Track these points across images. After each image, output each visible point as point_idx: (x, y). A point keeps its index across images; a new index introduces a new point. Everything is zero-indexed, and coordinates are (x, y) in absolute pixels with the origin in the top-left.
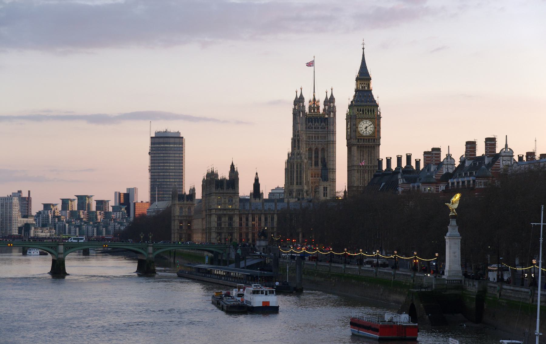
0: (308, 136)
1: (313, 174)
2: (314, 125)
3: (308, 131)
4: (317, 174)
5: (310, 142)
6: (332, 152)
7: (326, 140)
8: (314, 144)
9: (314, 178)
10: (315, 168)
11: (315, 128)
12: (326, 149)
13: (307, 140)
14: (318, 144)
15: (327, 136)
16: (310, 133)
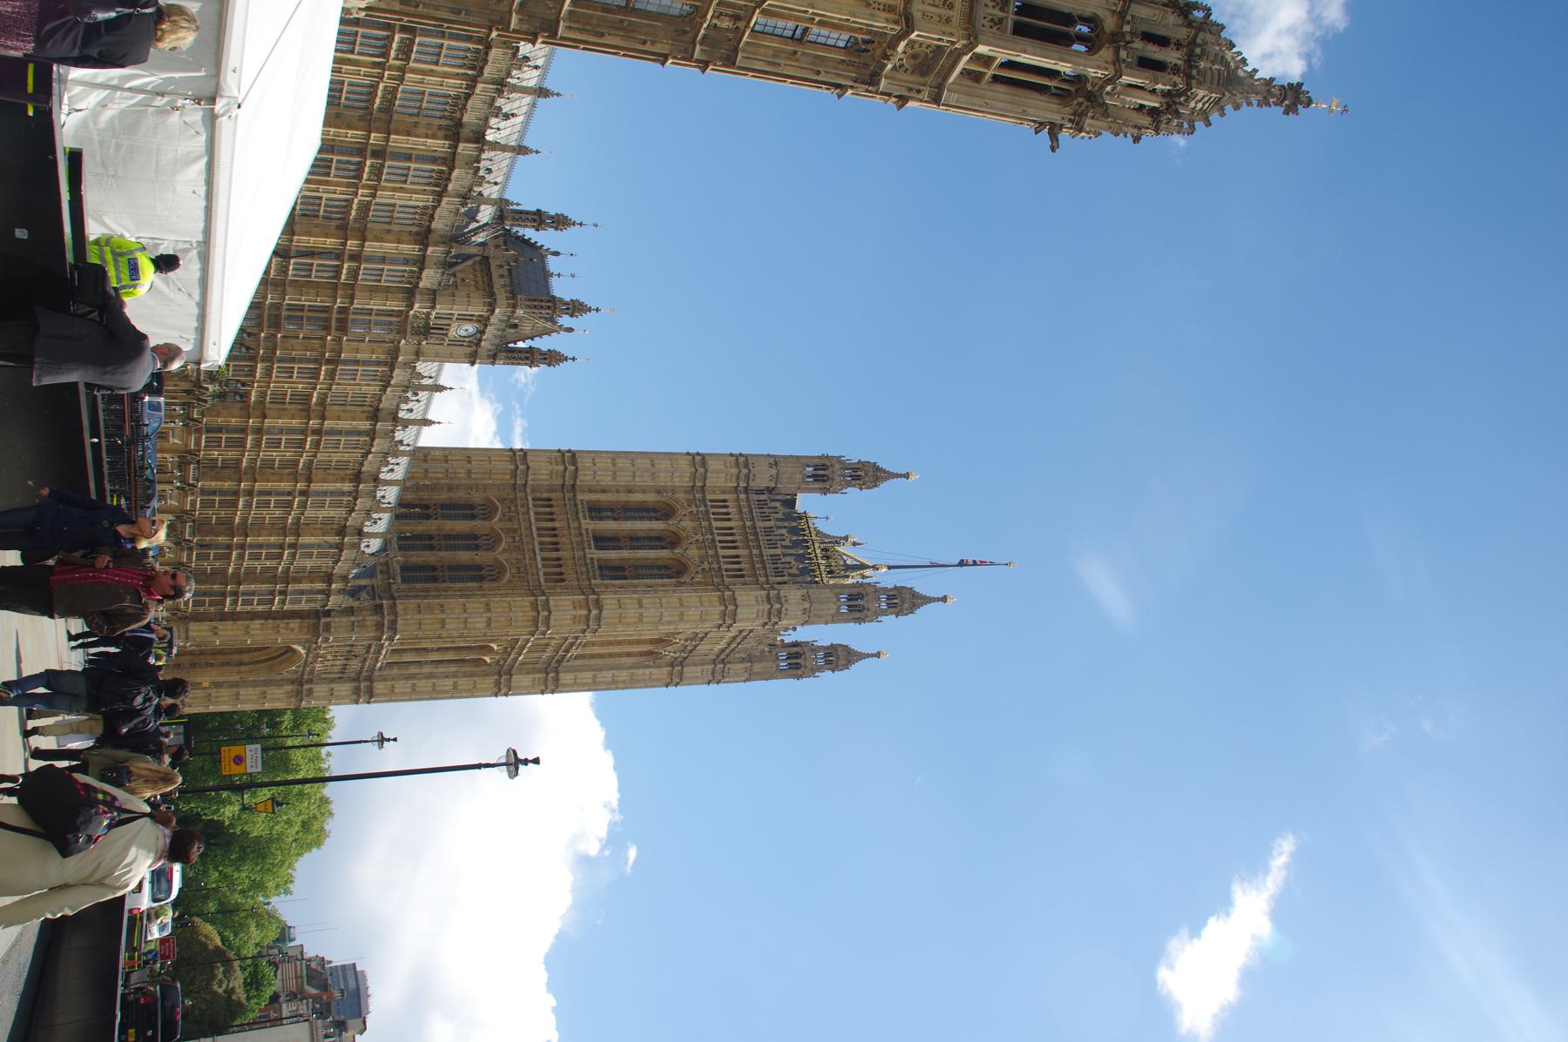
0: (725, 501)
1: (556, 524)
2: (780, 524)
3: (748, 500)
4: (557, 543)
5: (702, 509)
6: (681, 600)
7: (727, 580)
8: (694, 524)
9: (534, 529)
10: (584, 532)
11: (769, 531)
12: (688, 580)
13: (709, 497)
14: (701, 545)
15: (744, 584)
16: (739, 506)
